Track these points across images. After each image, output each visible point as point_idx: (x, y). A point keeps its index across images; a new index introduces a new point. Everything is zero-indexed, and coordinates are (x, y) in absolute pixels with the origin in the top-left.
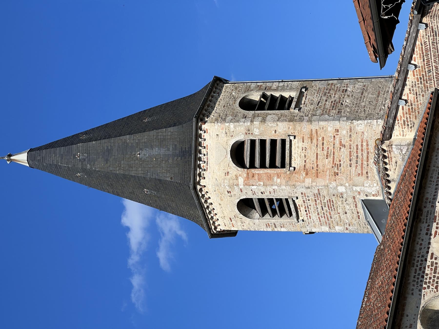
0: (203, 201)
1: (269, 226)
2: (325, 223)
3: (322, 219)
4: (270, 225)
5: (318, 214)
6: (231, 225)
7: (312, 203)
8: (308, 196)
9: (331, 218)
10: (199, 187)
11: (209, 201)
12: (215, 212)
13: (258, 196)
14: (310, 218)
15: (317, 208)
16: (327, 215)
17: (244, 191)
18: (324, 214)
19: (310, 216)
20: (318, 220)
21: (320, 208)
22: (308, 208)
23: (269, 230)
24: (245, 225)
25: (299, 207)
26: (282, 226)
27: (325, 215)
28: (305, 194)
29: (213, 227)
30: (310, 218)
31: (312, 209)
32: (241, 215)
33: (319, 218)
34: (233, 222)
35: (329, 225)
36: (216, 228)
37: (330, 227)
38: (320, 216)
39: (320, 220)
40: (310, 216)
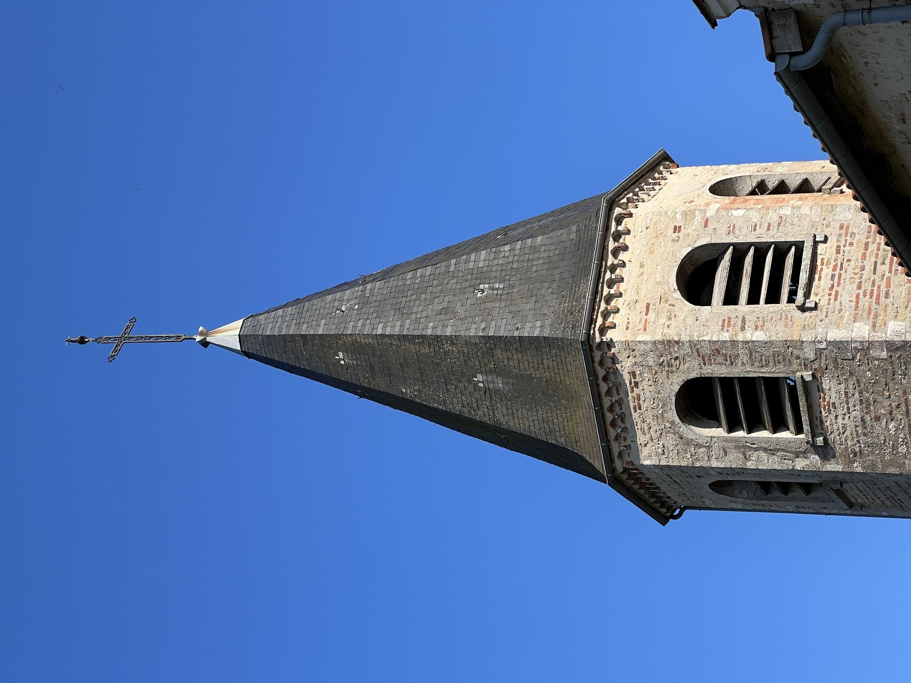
0: (611, 245)
1: (729, 325)
2: (865, 314)
3: (865, 302)
5: (859, 287)
6: (642, 327)
8: (853, 234)
9: (887, 295)
10: (617, 211)
11: (623, 256)
12: (622, 287)
13: (737, 238)
14: (836, 299)
15: (863, 269)
16: (879, 287)
17: (711, 226)
18: (873, 285)
19: (837, 292)
20: (854, 304)
21: (869, 266)
22: (841, 269)
23: (726, 336)
24: (673, 325)
25: (819, 268)
26: (760, 324)
27: (876, 288)
28: (848, 228)
29: (600, 321)
30: (836, 299)
31: (850, 269)
32: (678, 295)
33: (858, 296)
34: (652, 315)
35: (876, 316)
36: (603, 331)
37: (874, 326)
38: (861, 292)
39: (857, 302)
40: (837, 292)
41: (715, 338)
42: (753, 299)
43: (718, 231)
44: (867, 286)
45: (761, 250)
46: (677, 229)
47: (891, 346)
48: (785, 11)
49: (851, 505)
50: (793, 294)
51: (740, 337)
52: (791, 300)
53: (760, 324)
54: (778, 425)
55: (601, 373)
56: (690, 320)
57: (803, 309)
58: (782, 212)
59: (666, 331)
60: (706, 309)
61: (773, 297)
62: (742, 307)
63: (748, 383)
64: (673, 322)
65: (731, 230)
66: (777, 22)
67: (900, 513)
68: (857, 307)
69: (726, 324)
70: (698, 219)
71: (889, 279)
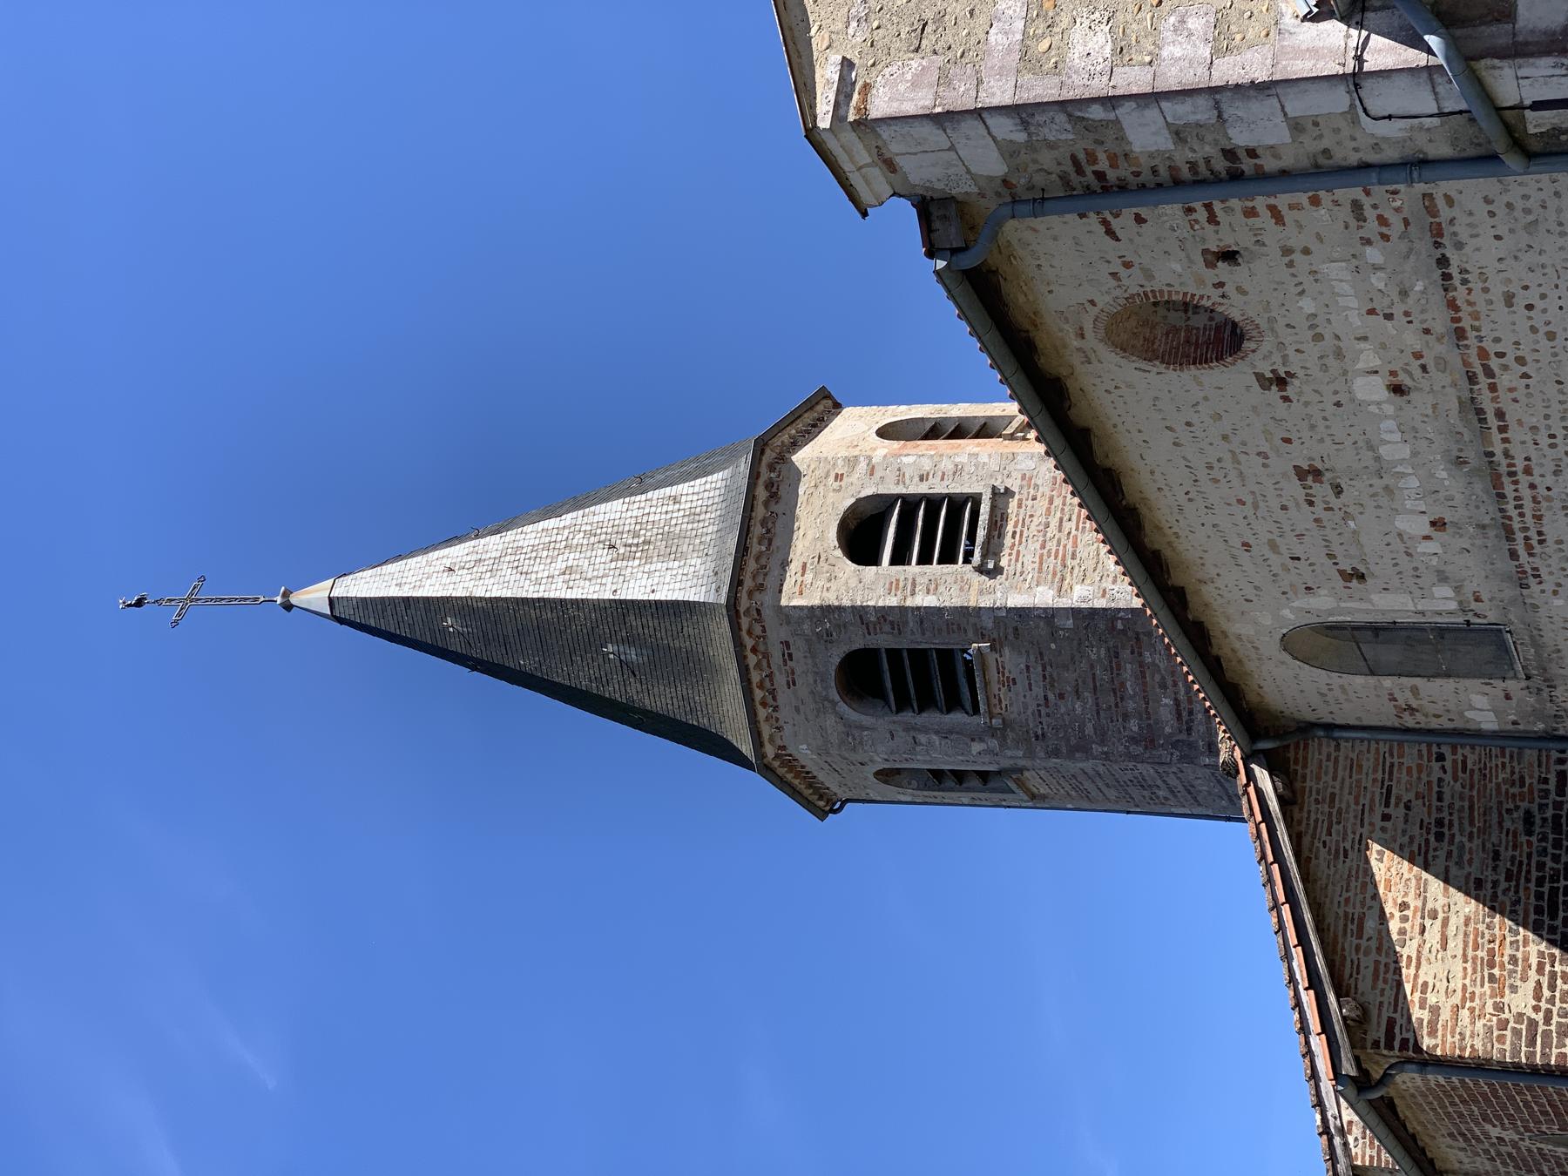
4: (901, 584)
5: (1043, 547)
6: (797, 589)
7: (1042, 504)
8: (1036, 486)
9: (1074, 557)
10: (769, 456)
15: (1047, 525)
17: (878, 474)
21: (1054, 522)
23: (893, 601)
26: (932, 587)
32: (839, 553)
33: (1041, 556)
34: (809, 576)
35: (1063, 579)
41: (880, 604)
42: (925, 559)
43: (887, 480)
44: (1052, 545)
45: (933, 503)
46: (839, 477)
47: (1075, 612)
48: (947, 200)
49: (1033, 797)
50: (968, 556)
51: (909, 603)
52: (967, 561)
53: (932, 587)
54: (953, 704)
55: (749, 642)
56: (853, 583)
57: (981, 570)
58: (957, 460)
59: (825, 594)
60: (871, 570)
61: (948, 557)
62: (913, 569)
63: (919, 656)
64: (833, 585)
65: (900, 478)
66: (935, 212)
67: (1086, 805)
68: (1040, 569)
69: (893, 587)
70: (863, 465)
71: (1076, 537)
